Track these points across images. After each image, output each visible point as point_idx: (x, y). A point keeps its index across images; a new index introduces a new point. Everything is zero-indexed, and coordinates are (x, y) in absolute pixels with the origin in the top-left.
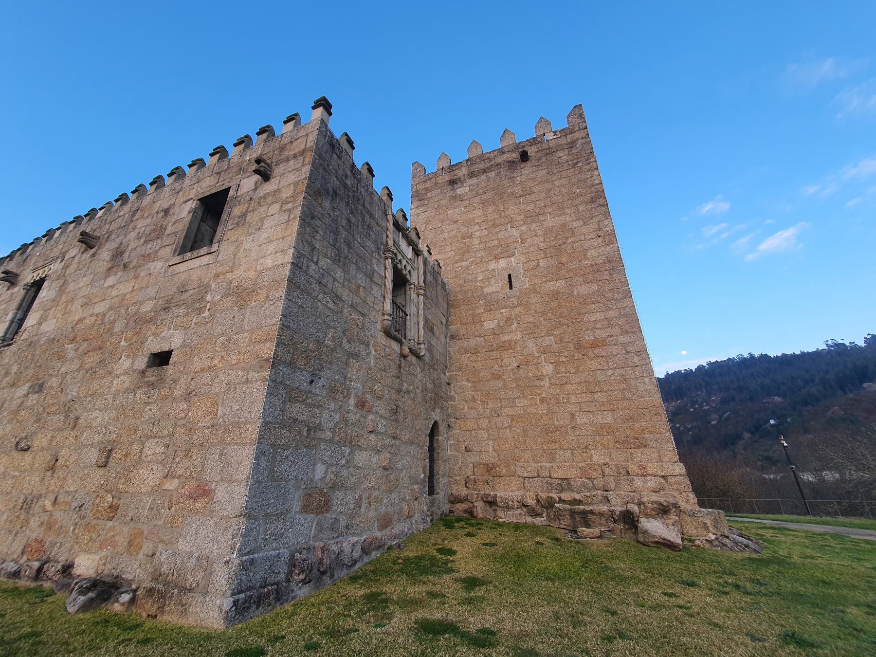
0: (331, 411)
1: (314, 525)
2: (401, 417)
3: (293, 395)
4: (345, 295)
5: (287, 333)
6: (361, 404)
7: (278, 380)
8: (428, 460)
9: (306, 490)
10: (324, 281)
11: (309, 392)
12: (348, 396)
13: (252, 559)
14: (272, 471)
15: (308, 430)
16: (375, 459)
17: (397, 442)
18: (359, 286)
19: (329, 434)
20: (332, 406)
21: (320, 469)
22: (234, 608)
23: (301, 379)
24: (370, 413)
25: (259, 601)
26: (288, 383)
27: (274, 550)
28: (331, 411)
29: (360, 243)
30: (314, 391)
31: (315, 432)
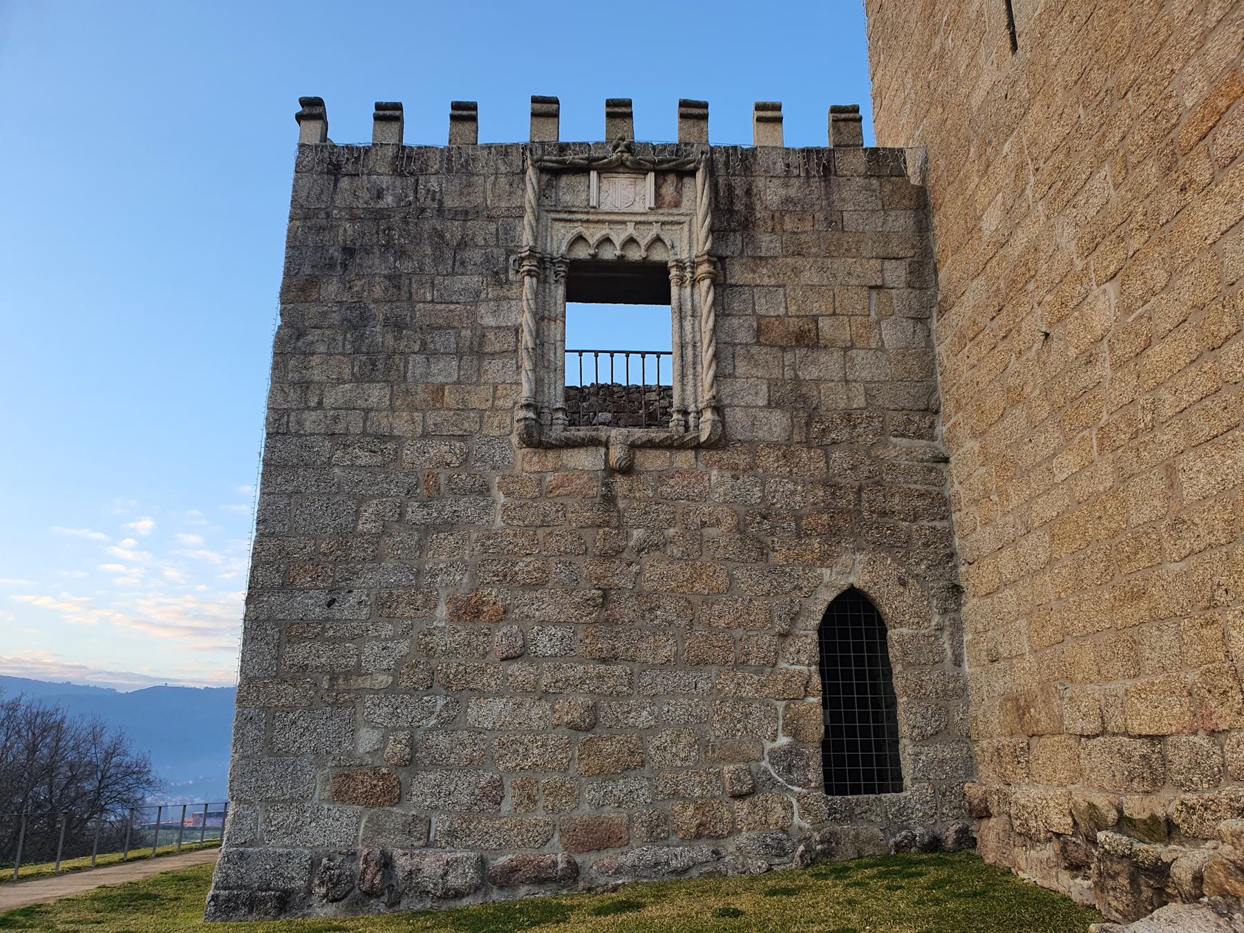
0: (386, 640)
1: (364, 821)
2: (626, 609)
3: (292, 632)
4: (401, 424)
5: (272, 544)
6: (469, 611)
7: (262, 617)
8: (815, 700)
9: (338, 770)
10: (340, 428)
11: (327, 619)
12: (430, 603)
13: (242, 853)
14: (269, 741)
15: (331, 680)
16: (537, 712)
17: (618, 669)
18: (441, 387)
19: (384, 680)
20: (388, 630)
21: (367, 739)
22: (212, 903)
23: (310, 604)
24: (501, 624)
25: (252, 904)
26: (281, 616)
27: (286, 847)
28: (386, 640)
29: (432, 301)
30: (338, 616)
31: (346, 679)
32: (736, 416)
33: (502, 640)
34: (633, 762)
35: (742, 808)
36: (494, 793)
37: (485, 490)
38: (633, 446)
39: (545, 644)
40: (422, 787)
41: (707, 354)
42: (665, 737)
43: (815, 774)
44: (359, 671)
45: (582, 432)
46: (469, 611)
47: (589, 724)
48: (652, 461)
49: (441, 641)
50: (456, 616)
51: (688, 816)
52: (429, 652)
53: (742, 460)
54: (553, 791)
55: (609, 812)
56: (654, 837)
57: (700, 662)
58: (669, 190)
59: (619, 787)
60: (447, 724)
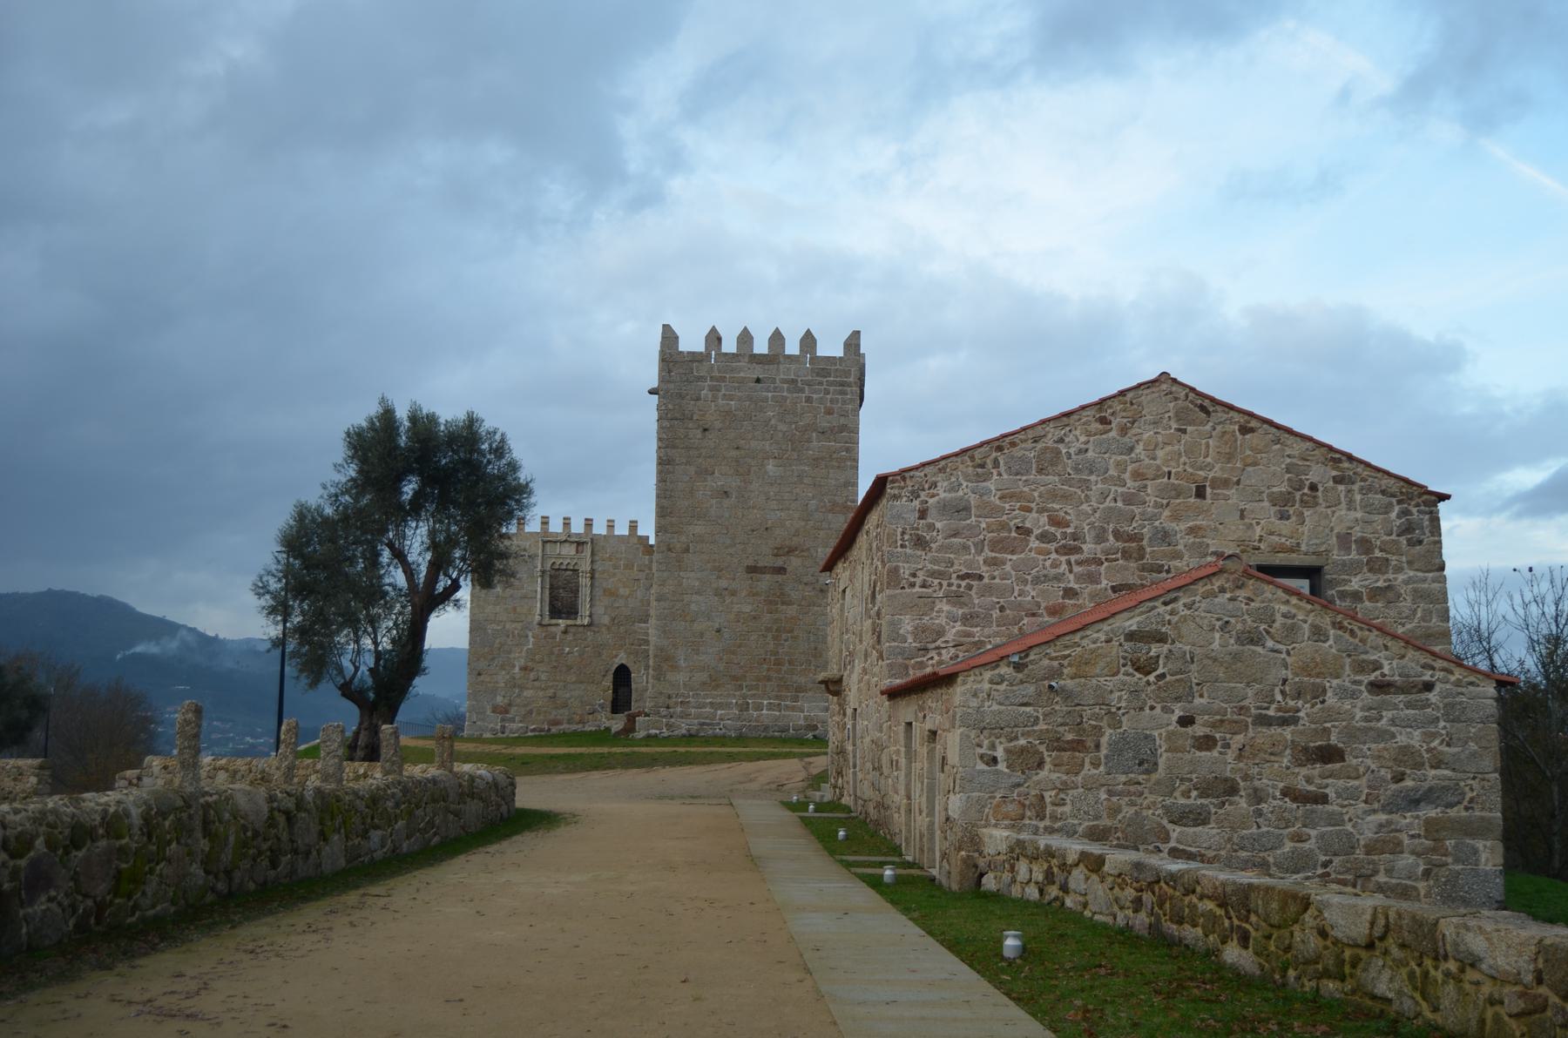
12: (514, 666)
16: (541, 694)
32: (595, 617)
33: (532, 676)
34: (565, 705)
35: (591, 717)
36: (531, 712)
37: (527, 636)
38: (567, 626)
39: (543, 677)
40: (513, 710)
41: (588, 600)
42: (572, 700)
43: (609, 709)
44: (497, 682)
45: (554, 621)
46: (524, 669)
47: (554, 697)
48: (572, 630)
49: (517, 677)
50: (521, 669)
51: (577, 718)
52: (514, 678)
53: (596, 629)
54: (545, 712)
55: (559, 717)
56: (569, 723)
57: (582, 682)
58: (580, 548)
59: (561, 711)
60: (519, 696)
